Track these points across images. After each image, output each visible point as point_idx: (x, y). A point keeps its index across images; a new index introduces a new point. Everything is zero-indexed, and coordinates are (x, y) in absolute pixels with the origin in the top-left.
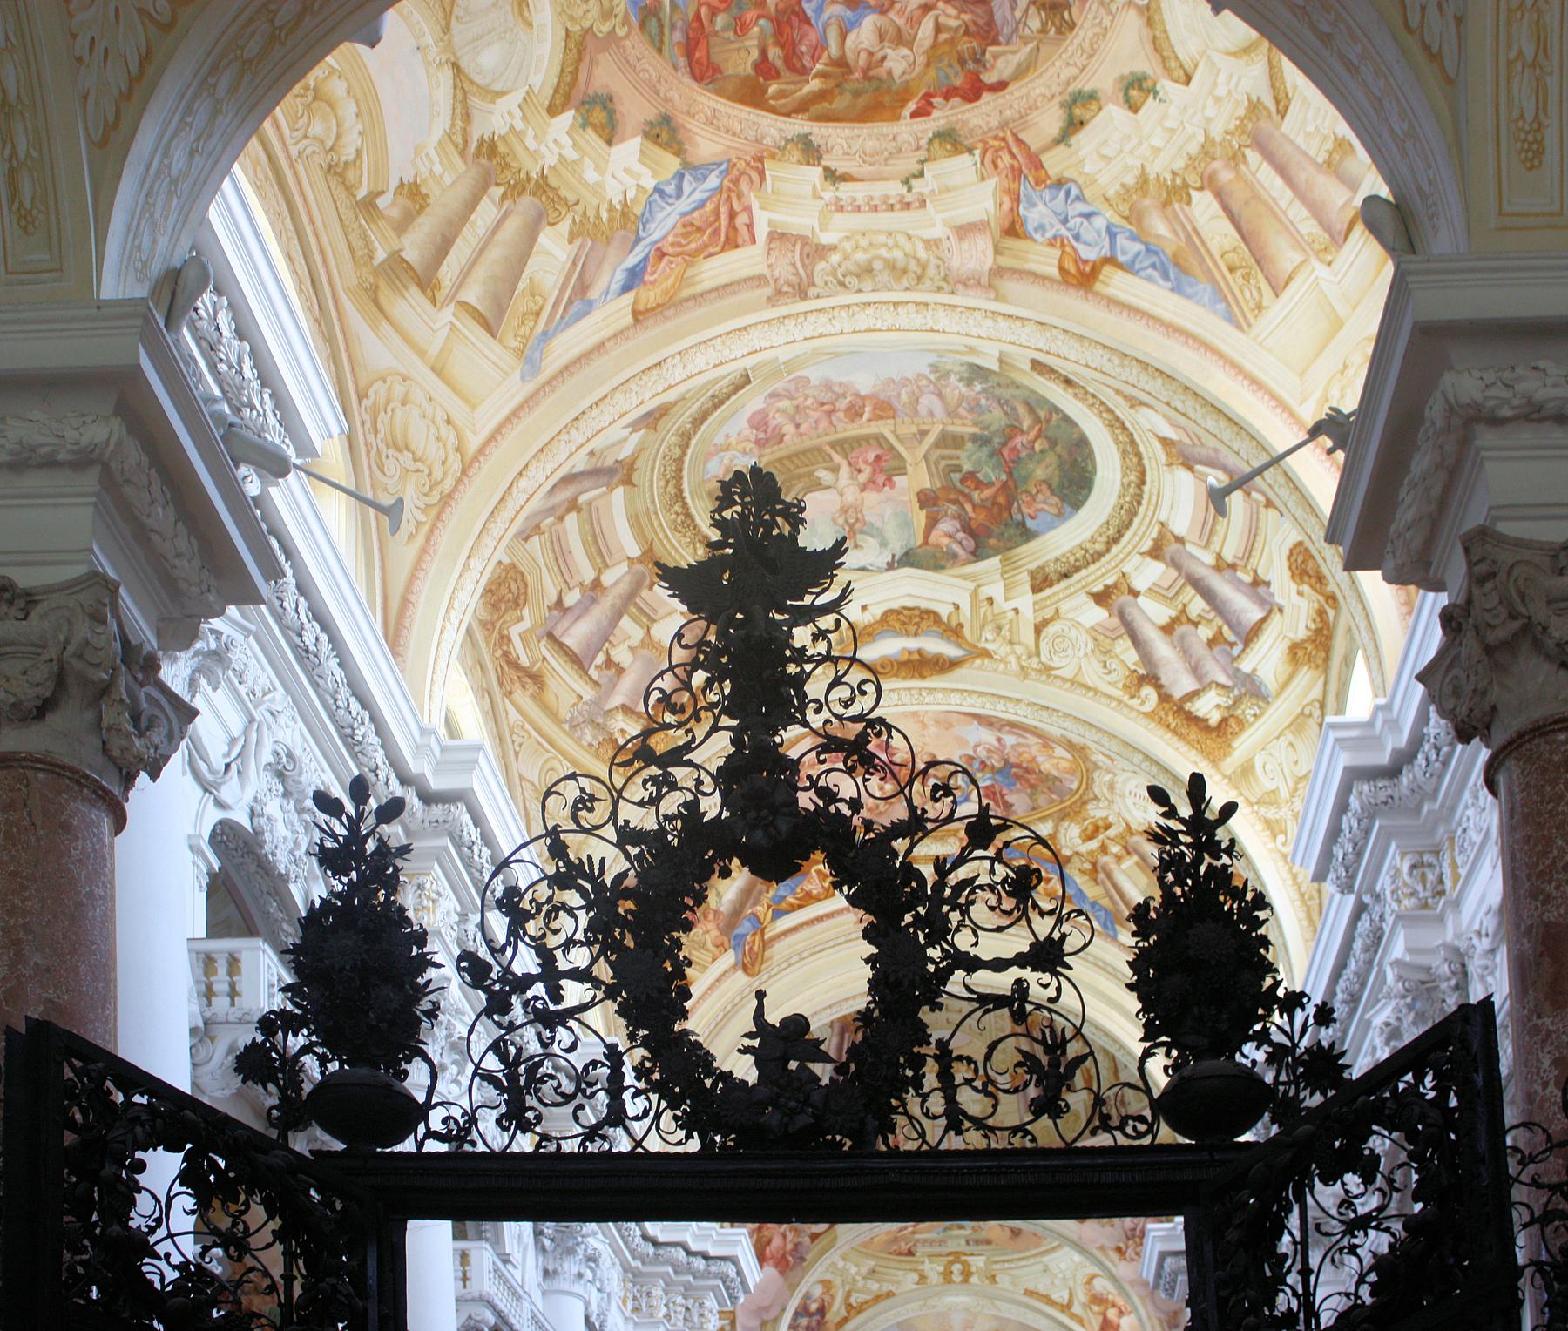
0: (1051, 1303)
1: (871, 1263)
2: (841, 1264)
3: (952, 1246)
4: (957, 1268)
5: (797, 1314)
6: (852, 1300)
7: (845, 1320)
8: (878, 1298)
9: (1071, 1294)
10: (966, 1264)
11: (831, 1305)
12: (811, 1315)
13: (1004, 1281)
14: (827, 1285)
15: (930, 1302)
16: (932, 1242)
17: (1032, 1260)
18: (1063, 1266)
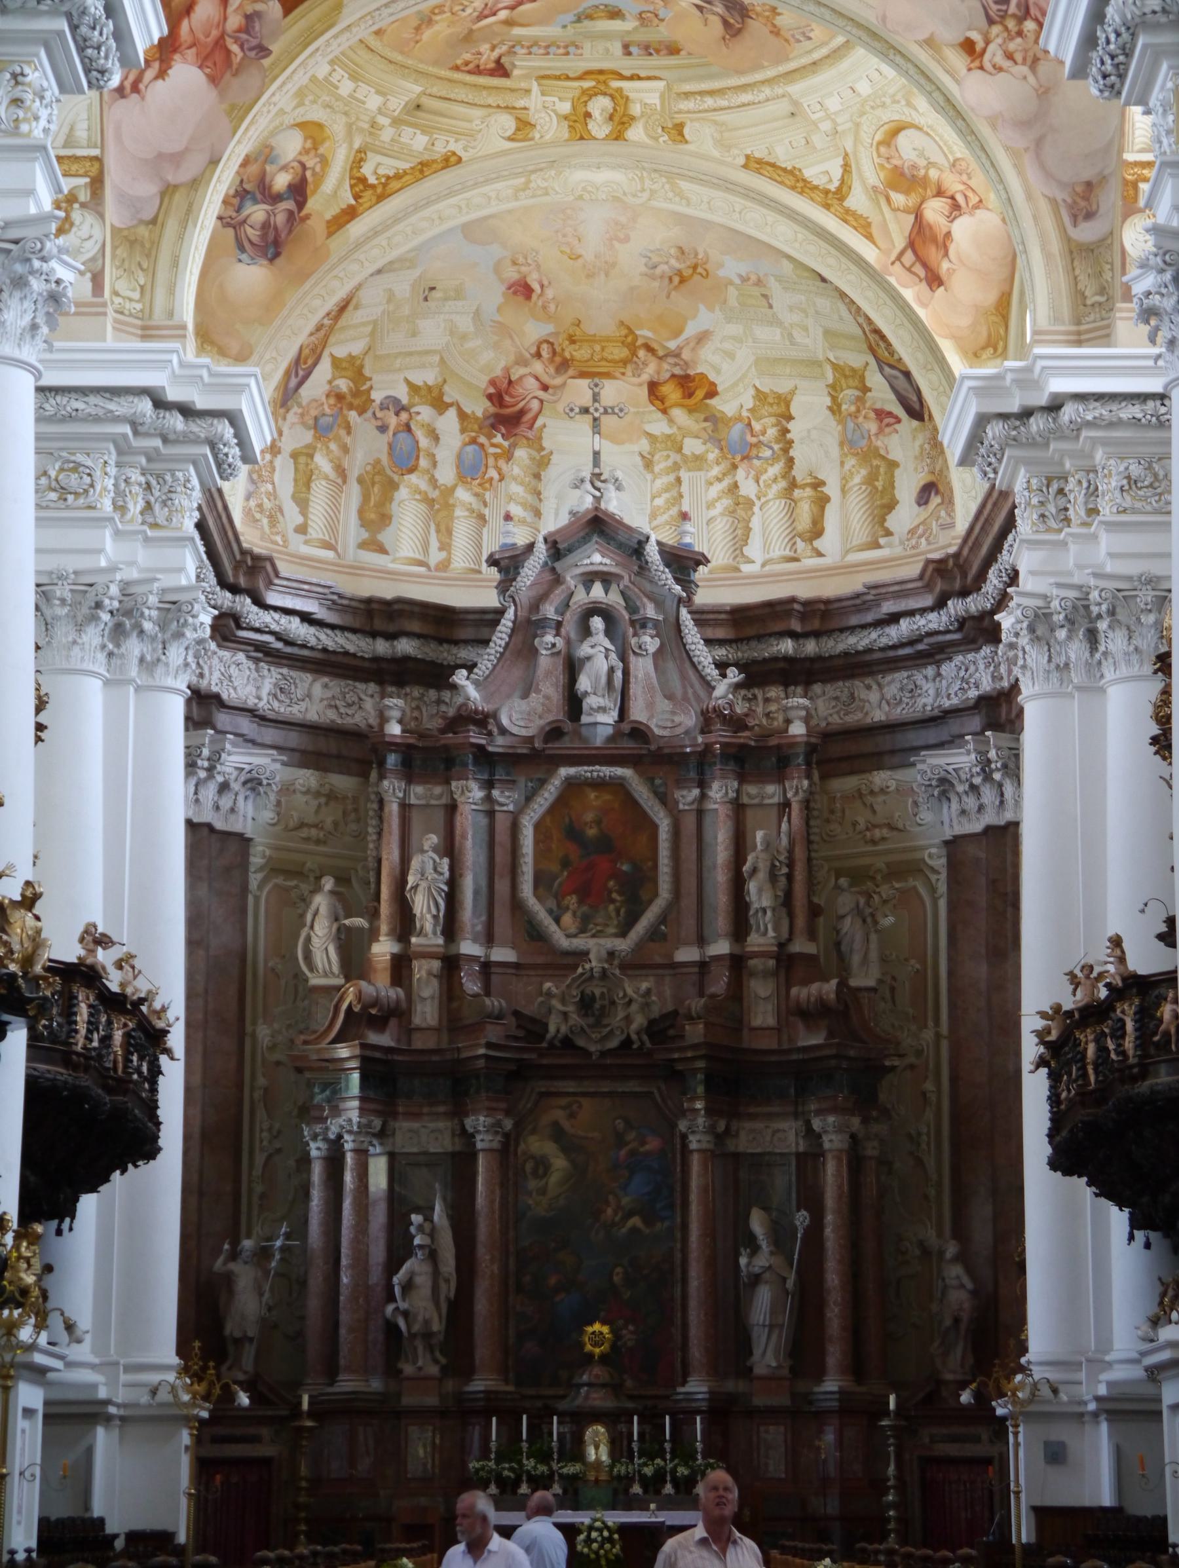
0: (802, 186)
1: (414, 89)
2: (346, 87)
3: (593, 57)
4: (600, 106)
5: (240, 196)
6: (367, 170)
7: (350, 214)
8: (423, 169)
9: (846, 168)
10: (620, 99)
11: (320, 178)
12: (276, 198)
13: (700, 135)
14: (314, 132)
15: (537, 181)
16: (548, 47)
17: (767, 91)
18: (833, 104)
